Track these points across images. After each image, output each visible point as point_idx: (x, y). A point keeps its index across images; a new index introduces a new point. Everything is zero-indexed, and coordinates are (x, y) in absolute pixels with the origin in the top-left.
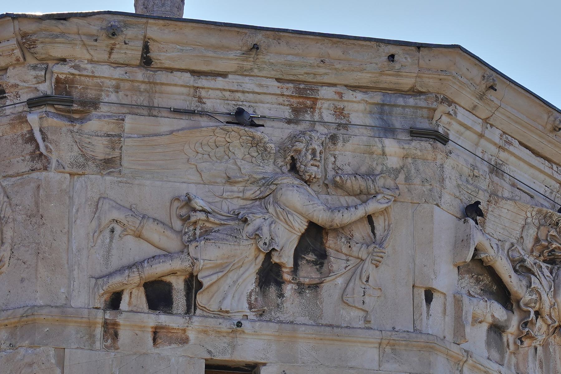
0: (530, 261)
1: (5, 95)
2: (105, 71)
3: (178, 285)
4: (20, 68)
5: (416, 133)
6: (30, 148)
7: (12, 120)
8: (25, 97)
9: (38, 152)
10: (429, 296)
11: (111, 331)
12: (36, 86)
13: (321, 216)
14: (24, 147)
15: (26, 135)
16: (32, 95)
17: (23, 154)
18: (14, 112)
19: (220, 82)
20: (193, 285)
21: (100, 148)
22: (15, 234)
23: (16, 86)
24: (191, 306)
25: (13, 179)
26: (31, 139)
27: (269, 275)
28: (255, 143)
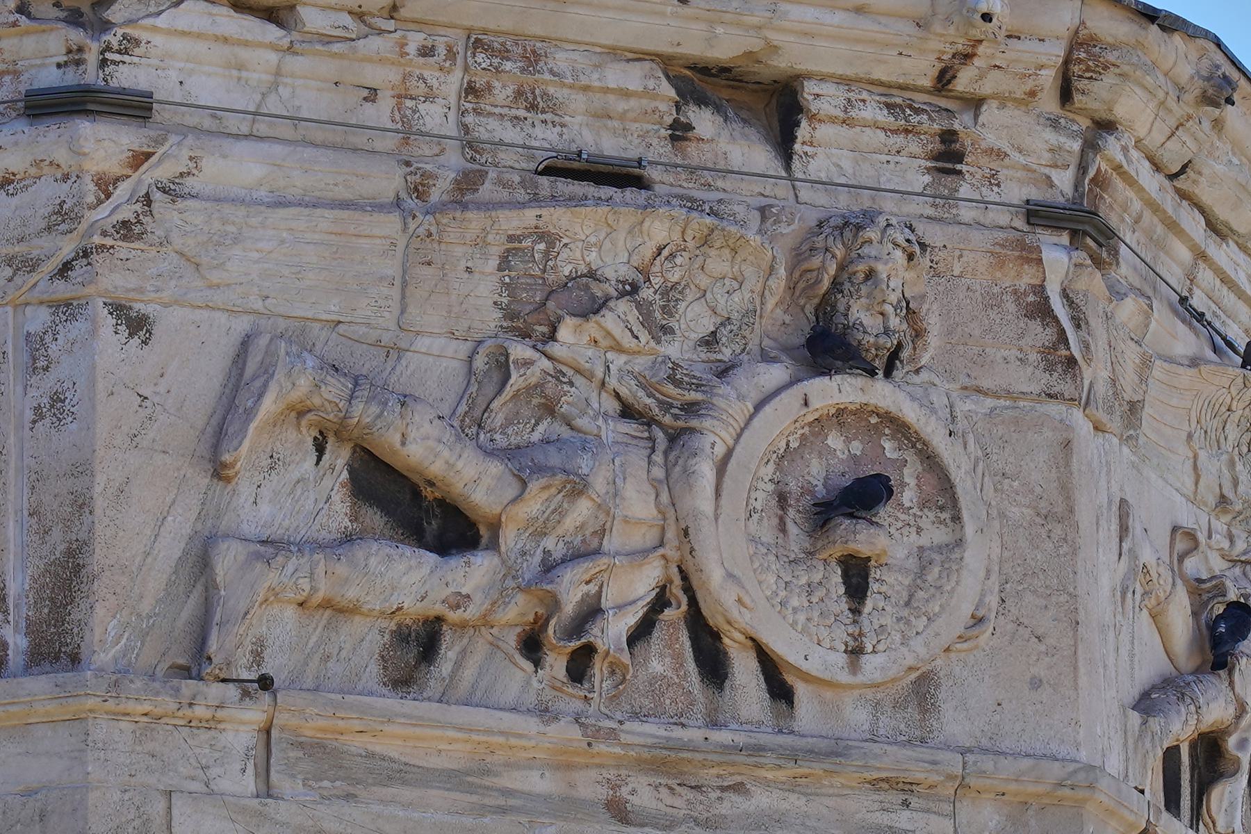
1: (958, 167)
4: (1017, 112)
6: (1040, 334)
7: (1002, 246)
8: (1016, 192)
9: (1064, 352)
12: (1047, 171)
14: (1022, 325)
15: (1025, 294)
16: (1035, 194)
17: (1022, 343)
18: (982, 220)
22: (1006, 554)
23: (1001, 155)
25: (990, 402)
26: (1042, 311)
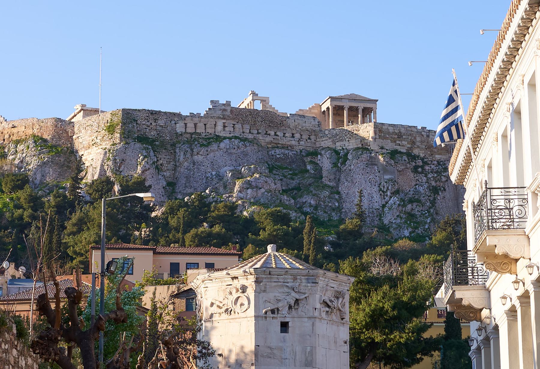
0: (333, 299)
2: (263, 276)
3: (276, 310)
5: (313, 283)
10: (315, 309)
11: (266, 317)
13: (298, 297)
19: (282, 277)
20: (278, 309)
21: (263, 289)
24: (278, 313)
27: (290, 307)
28: (287, 286)
